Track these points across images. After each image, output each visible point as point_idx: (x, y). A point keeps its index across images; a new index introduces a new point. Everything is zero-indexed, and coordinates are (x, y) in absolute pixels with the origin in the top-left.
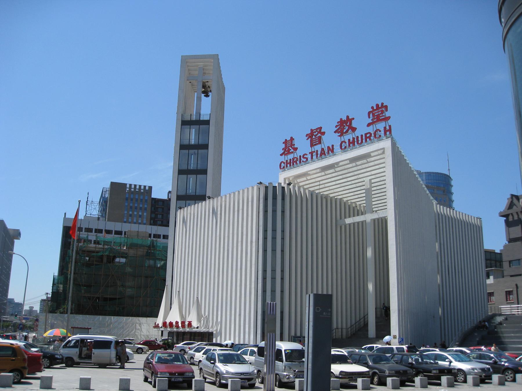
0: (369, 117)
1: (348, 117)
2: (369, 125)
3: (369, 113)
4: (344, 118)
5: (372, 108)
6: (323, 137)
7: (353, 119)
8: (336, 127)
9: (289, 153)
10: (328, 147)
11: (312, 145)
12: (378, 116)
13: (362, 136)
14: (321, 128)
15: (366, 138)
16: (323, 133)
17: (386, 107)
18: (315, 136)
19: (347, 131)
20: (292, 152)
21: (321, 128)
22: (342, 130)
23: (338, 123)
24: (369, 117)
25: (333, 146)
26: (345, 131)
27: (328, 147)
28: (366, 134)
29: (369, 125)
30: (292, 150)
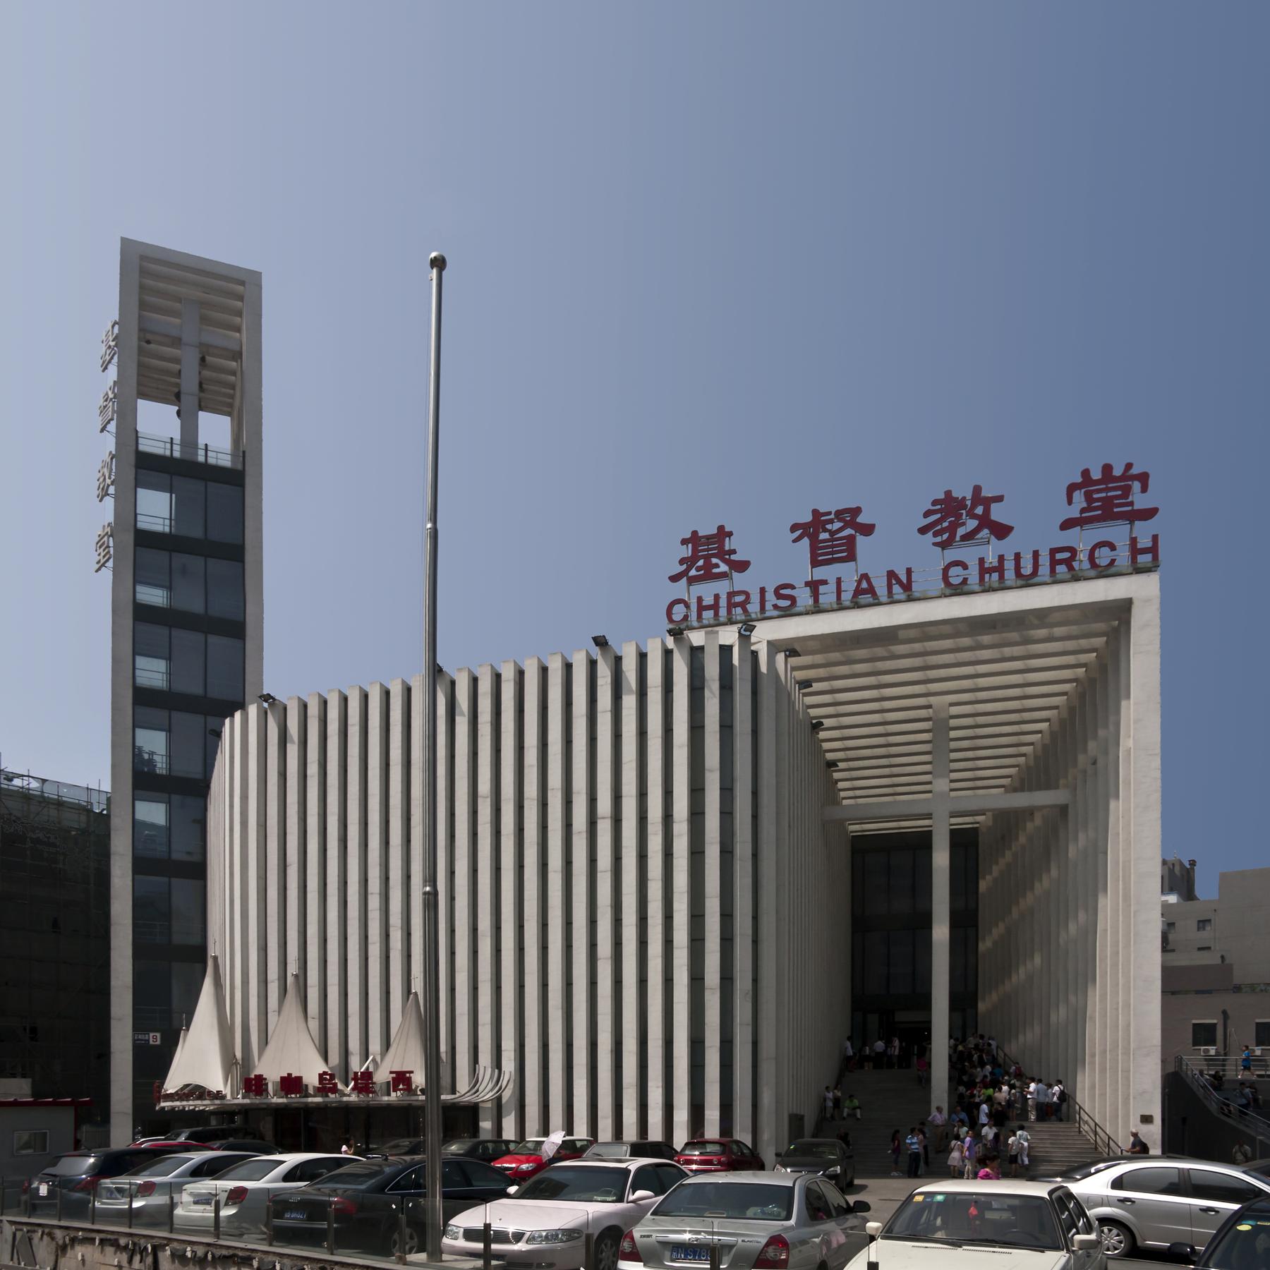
0: (1070, 502)
1: (977, 489)
2: (1067, 525)
3: (1072, 489)
4: (963, 491)
5: (1086, 473)
6: (860, 539)
7: (999, 499)
8: (927, 514)
9: (708, 575)
10: (891, 575)
11: (815, 563)
12: (1108, 503)
13: (1036, 555)
14: (857, 511)
15: (1054, 563)
16: (868, 530)
17: (1144, 478)
18: (832, 533)
19: (968, 537)
20: (723, 575)
21: (857, 511)
22: (952, 529)
23: (935, 503)
24: (1070, 502)
25: (909, 571)
26: (961, 531)
27: (891, 575)
28: (1053, 551)
29: (1067, 525)
30: (723, 568)
